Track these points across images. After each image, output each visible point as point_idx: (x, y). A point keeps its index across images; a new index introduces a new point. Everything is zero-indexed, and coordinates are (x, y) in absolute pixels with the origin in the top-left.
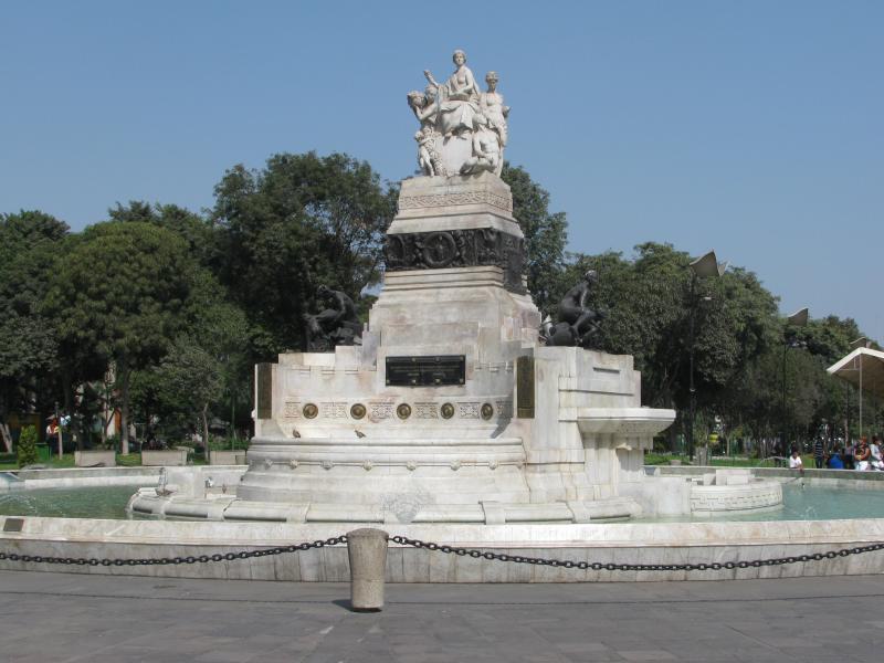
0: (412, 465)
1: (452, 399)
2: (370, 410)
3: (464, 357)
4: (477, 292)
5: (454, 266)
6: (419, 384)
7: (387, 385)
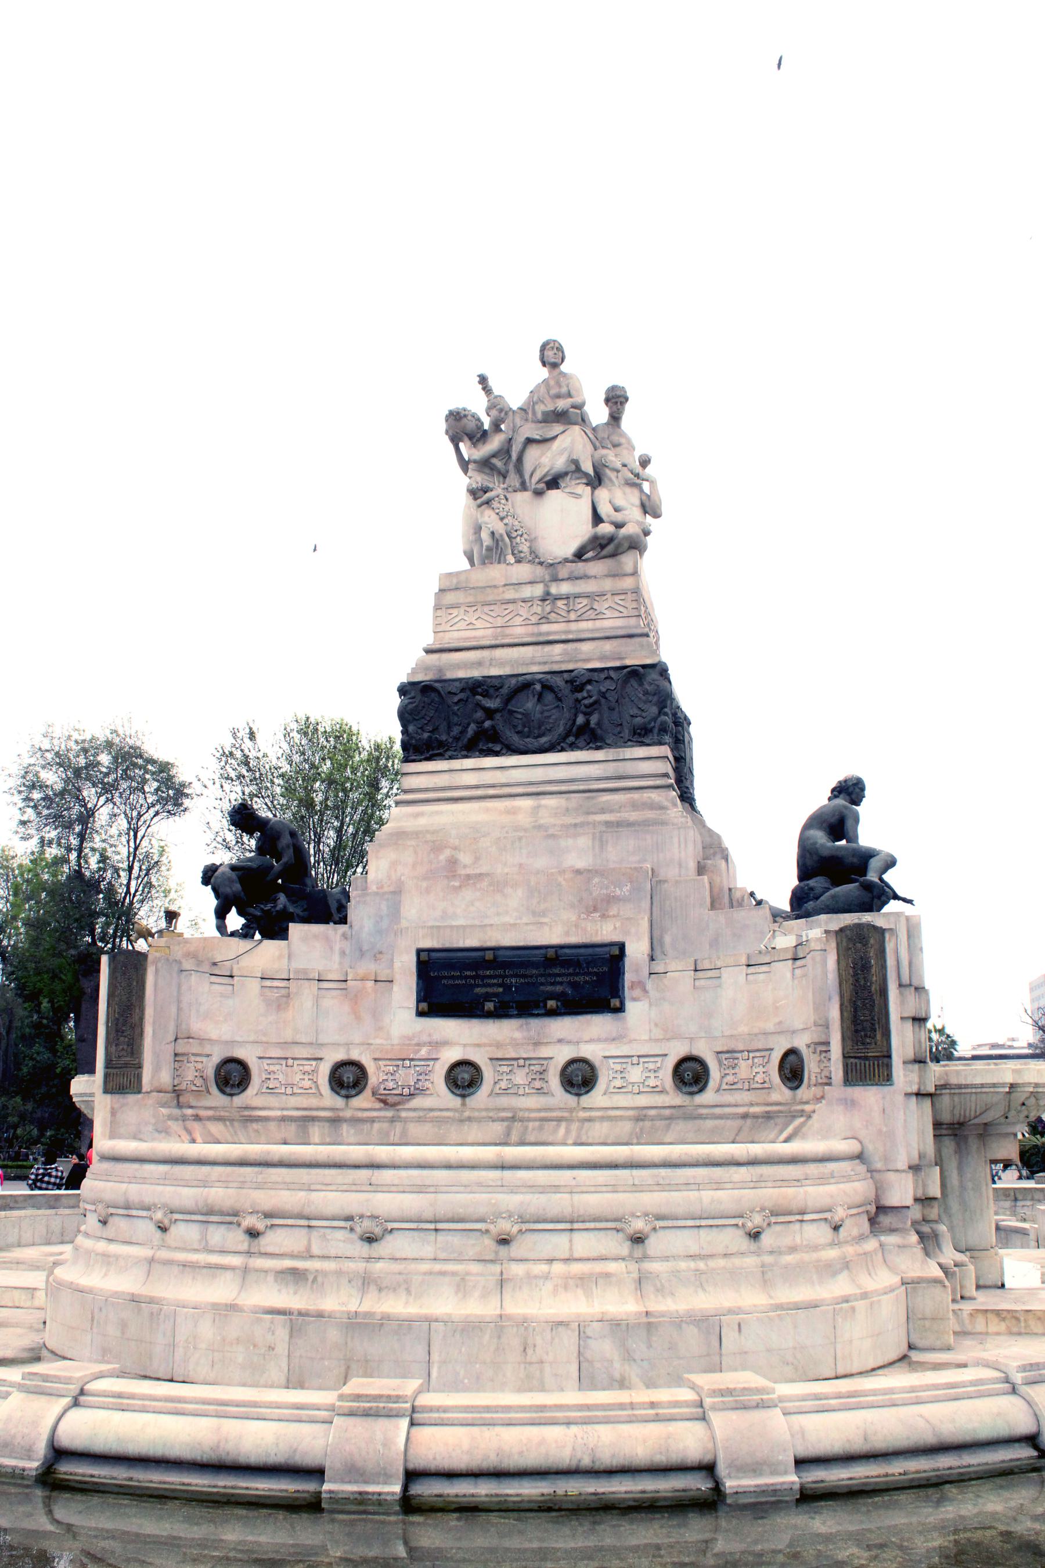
0: (639, 1225)
1: (589, 1051)
2: (374, 1077)
3: (622, 947)
4: (635, 806)
5: (573, 747)
6: (500, 1013)
7: (420, 1014)
